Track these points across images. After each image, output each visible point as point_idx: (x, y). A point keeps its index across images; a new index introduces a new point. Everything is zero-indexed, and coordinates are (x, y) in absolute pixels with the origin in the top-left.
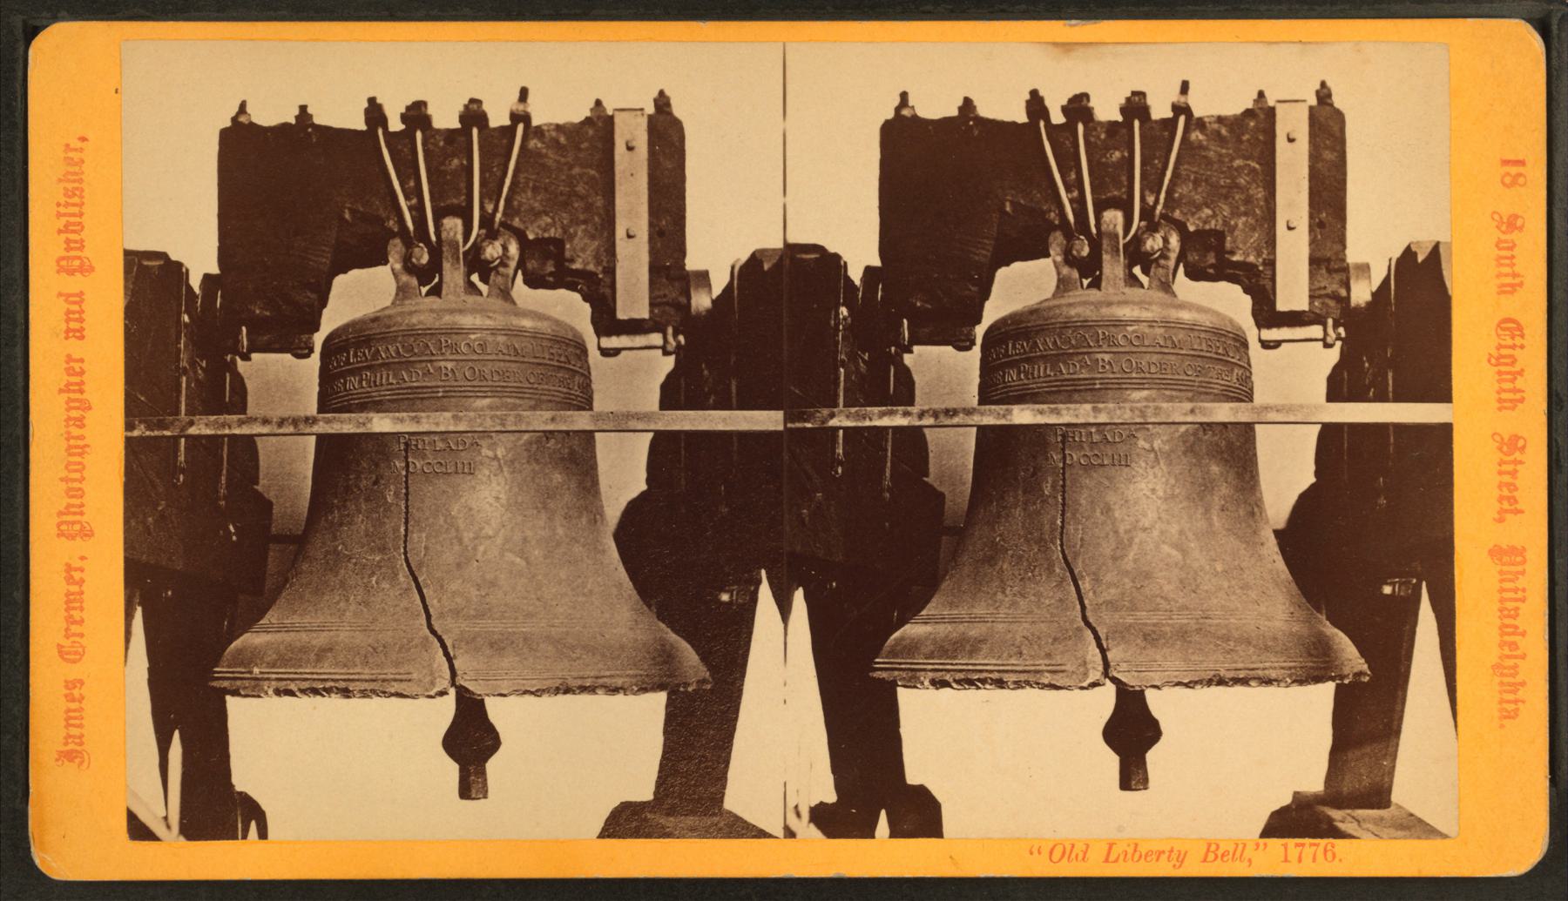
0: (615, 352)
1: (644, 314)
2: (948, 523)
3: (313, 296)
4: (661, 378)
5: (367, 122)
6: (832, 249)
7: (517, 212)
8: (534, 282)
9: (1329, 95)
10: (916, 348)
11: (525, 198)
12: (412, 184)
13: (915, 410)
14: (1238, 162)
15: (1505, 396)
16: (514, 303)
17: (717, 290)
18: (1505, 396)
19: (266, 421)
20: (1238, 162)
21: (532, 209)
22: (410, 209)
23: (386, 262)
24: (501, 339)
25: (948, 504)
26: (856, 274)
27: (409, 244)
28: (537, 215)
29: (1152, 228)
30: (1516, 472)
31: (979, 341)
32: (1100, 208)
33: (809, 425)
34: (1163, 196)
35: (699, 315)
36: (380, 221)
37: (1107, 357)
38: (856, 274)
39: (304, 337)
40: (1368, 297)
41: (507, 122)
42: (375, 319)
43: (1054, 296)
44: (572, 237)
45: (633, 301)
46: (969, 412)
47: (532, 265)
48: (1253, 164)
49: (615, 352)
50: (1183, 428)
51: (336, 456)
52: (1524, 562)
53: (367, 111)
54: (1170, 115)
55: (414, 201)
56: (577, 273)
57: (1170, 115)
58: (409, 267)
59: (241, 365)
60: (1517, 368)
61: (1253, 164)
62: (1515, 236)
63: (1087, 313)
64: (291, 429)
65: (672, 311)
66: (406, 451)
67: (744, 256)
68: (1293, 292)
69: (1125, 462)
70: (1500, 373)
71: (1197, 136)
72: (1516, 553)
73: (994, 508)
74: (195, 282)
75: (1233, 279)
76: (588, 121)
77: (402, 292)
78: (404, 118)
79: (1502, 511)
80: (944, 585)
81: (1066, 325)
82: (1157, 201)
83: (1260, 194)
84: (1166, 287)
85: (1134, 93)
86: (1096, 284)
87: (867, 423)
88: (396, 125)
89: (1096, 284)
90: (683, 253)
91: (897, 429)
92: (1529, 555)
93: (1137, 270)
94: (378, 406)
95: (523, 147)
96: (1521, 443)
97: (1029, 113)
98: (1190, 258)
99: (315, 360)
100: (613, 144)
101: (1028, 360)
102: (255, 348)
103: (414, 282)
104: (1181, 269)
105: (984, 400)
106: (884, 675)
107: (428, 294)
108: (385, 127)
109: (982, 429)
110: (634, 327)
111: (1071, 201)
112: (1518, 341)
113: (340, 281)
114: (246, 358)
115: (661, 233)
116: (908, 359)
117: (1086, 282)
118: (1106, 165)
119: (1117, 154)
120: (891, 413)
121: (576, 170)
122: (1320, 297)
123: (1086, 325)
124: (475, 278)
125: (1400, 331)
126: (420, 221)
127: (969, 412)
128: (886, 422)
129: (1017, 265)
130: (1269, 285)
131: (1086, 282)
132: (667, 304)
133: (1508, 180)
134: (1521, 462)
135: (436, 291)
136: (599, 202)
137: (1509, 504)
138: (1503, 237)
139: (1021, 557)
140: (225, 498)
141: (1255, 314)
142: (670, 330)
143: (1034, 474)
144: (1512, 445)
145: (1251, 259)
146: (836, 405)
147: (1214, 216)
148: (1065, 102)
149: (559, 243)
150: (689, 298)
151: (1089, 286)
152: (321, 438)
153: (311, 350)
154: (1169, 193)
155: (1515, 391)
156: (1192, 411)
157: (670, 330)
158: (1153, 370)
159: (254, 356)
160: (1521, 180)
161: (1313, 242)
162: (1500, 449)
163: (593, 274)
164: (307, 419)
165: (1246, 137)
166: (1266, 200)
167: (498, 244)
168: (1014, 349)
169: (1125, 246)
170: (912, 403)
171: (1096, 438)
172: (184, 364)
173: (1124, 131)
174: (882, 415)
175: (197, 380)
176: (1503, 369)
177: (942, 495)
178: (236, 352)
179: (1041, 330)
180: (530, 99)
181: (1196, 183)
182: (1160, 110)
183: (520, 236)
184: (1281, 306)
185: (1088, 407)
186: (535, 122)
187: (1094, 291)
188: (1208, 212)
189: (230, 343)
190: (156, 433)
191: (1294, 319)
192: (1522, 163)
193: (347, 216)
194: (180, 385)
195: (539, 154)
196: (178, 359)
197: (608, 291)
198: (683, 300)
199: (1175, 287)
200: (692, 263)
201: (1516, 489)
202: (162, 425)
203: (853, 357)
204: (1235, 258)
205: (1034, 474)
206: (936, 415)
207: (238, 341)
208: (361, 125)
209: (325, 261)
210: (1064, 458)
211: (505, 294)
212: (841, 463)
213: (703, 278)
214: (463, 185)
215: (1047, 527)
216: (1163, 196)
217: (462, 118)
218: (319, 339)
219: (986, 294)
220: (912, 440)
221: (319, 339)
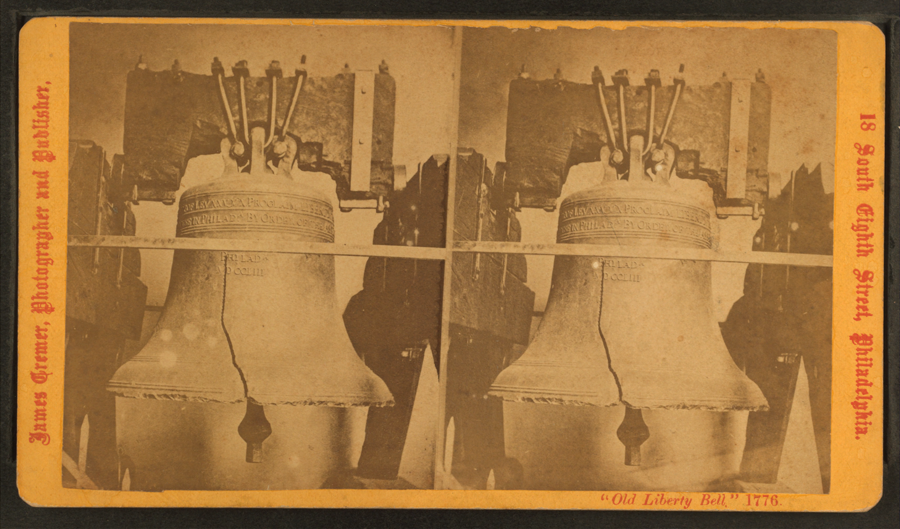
0: (350, 209)
1: (366, 188)
2: (536, 309)
3: (177, 170)
4: (376, 226)
5: (213, 71)
6: (478, 152)
7: (297, 126)
8: (304, 167)
9: (763, 77)
10: (523, 209)
11: (301, 119)
12: (237, 107)
13: (520, 244)
14: (709, 113)
15: (861, 248)
16: (292, 178)
17: (410, 175)
18: (861, 248)
19: (146, 240)
20: (709, 113)
21: (305, 125)
22: (235, 122)
23: (219, 152)
24: (283, 199)
25: (536, 299)
26: (492, 167)
27: (233, 142)
28: (308, 129)
30: (867, 292)
31: (558, 207)
32: (631, 134)
33: (460, 250)
34: (666, 129)
35: (398, 191)
36: (218, 128)
37: (630, 220)
38: (492, 167)
39: (170, 193)
41: (294, 75)
42: (211, 185)
43: (602, 183)
44: (327, 142)
45: (360, 180)
46: (551, 247)
47: (303, 157)
48: (718, 114)
49: (350, 209)
50: (671, 262)
51: (184, 261)
52: (871, 343)
53: (213, 64)
54: (672, 83)
55: (237, 118)
56: (330, 163)
57: (672, 83)
58: (233, 155)
59: (133, 208)
60: (869, 232)
61: (718, 114)
62: (868, 157)
63: (620, 194)
64: (160, 246)
65: (383, 187)
66: (226, 261)
67: (424, 159)
68: (737, 188)
69: (637, 279)
70: (858, 235)
71: (686, 96)
72: (867, 338)
73: (562, 302)
74: (110, 159)
76: (340, 76)
77: (228, 169)
78: (234, 70)
79: (859, 314)
80: (532, 345)
81: (608, 201)
82: (662, 133)
83: (720, 130)
84: (665, 181)
85: (652, 71)
86: (626, 177)
87: (493, 250)
88: (229, 73)
89: (626, 177)
90: (391, 154)
91: (510, 255)
92: (874, 339)
94: (210, 234)
95: (302, 89)
96: (870, 276)
97: (593, 80)
98: (681, 165)
99: (176, 207)
100: (353, 89)
101: (585, 218)
102: (141, 198)
103: (235, 163)
104: (674, 170)
105: (558, 241)
106: (498, 394)
107: (243, 171)
108: (223, 75)
109: (559, 259)
110: (361, 196)
111: (615, 130)
112: (870, 217)
113: (192, 162)
114: (136, 203)
115: (379, 142)
116: (517, 213)
117: (620, 176)
118: (634, 111)
119: (641, 106)
120: (507, 245)
121: (332, 104)
122: (752, 191)
123: (619, 200)
124: (270, 163)
125: (800, 211)
126: (240, 130)
127: (551, 247)
128: (504, 250)
129: (583, 165)
130: (723, 183)
131: (620, 176)
132: (381, 183)
133: (865, 126)
134: (870, 287)
135: (248, 170)
136: (344, 123)
137: (863, 311)
138: (861, 157)
139: (576, 331)
140: (121, 283)
141: (714, 200)
142: (381, 198)
143: (585, 284)
144: (865, 276)
145: (714, 168)
146: (476, 239)
147: (695, 141)
148: (613, 74)
149: (320, 146)
150: (393, 180)
151: (622, 178)
152: (178, 252)
153: (174, 201)
154: (670, 129)
155: (867, 245)
156: (676, 252)
157: (381, 198)
158: (656, 227)
159: (141, 202)
160: (872, 127)
161: (750, 158)
162: (858, 278)
163: (339, 164)
164: (170, 240)
165: (715, 98)
166: (724, 134)
167: (284, 144)
168: (578, 212)
169: (644, 157)
170: (519, 240)
171: (622, 265)
172: (101, 205)
173: (645, 92)
174: (503, 246)
175: (108, 215)
176: (861, 233)
177: (533, 294)
179: (593, 202)
180: (307, 61)
181: (685, 122)
182: (667, 82)
183: (298, 140)
184: (730, 195)
185: (618, 247)
186: (309, 76)
188: (691, 139)
190: (83, 244)
192: (873, 117)
193: (199, 124)
194: (97, 217)
195: (311, 94)
196: (98, 202)
197: (347, 175)
198: (390, 182)
199: (670, 181)
200: (396, 161)
201: (867, 302)
202: (86, 239)
203: (488, 212)
204: (706, 166)
205: (585, 284)
206: (532, 248)
207: (131, 193)
208: (209, 73)
209: (184, 150)
210: (603, 275)
211: (287, 173)
212: (478, 273)
213: (403, 168)
214: (266, 110)
215: (591, 317)
216: (666, 129)
217: (267, 72)
218: (178, 195)
219: (563, 181)
220: (519, 261)
221: (178, 195)
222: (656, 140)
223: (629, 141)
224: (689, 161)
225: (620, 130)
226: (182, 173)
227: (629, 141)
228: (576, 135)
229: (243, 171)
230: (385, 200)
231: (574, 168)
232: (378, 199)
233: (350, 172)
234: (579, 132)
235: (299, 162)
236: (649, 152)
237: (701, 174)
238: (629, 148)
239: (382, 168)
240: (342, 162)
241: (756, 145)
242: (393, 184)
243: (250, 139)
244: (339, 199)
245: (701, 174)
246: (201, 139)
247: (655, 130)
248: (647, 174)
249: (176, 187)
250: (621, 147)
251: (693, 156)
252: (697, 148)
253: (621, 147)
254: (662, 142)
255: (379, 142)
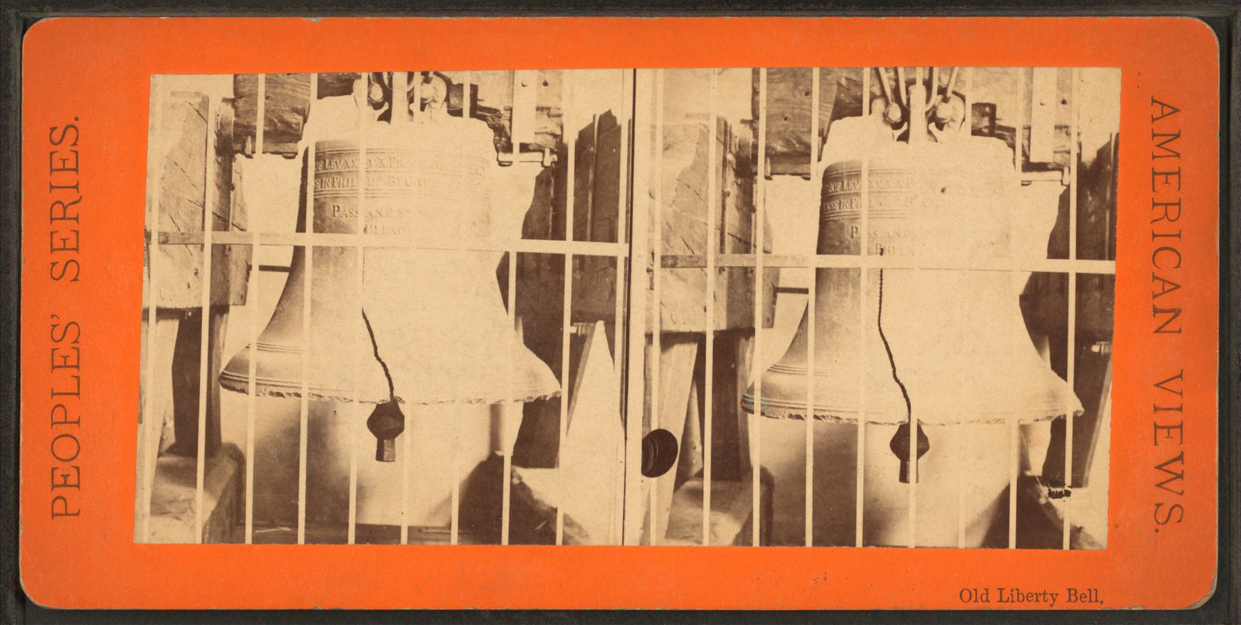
3: (301, 118)
29: (945, 100)
39: (292, 145)
40: (1094, 155)
65: (550, 138)
75: (1001, 137)
93: (932, 126)
107: (381, 118)
115: (545, 84)
142: (547, 151)
157: (547, 151)
163: (496, 111)
166: (1027, 84)
178: (242, 152)
187: (903, 143)
189: (238, 147)
191: (1042, 167)
198: (559, 132)
207: (244, 147)
222: (942, 91)
223: (908, 92)
224: (983, 115)
225: (897, 80)
226: (305, 121)
227: (908, 92)
228: (839, 84)
229: (381, 118)
230: (552, 152)
231: (836, 123)
232: (543, 152)
233: (510, 120)
234: (844, 82)
235: (449, 106)
236: (934, 107)
237: (997, 132)
238: (908, 100)
239: (549, 115)
240: (501, 108)
241: (1066, 97)
242: (562, 136)
243: (390, 80)
244: (498, 151)
245: (997, 132)
246: (329, 80)
247: (940, 79)
248: (930, 132)
249: (298, 138)
250: (898, 99)
251: (987, 109)
252: (992, 102)
253: (898, 99)
254: (949, 94)
255: (545, 84)
